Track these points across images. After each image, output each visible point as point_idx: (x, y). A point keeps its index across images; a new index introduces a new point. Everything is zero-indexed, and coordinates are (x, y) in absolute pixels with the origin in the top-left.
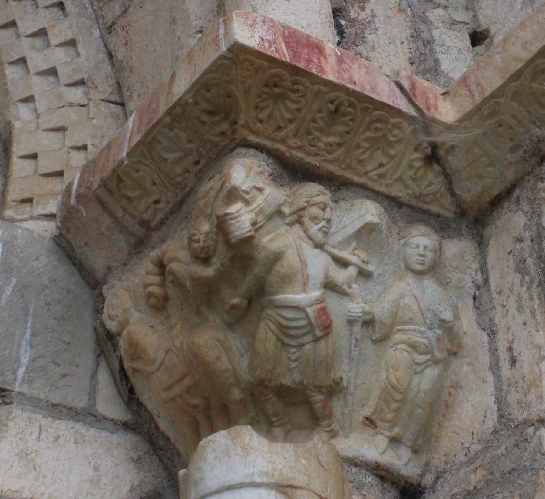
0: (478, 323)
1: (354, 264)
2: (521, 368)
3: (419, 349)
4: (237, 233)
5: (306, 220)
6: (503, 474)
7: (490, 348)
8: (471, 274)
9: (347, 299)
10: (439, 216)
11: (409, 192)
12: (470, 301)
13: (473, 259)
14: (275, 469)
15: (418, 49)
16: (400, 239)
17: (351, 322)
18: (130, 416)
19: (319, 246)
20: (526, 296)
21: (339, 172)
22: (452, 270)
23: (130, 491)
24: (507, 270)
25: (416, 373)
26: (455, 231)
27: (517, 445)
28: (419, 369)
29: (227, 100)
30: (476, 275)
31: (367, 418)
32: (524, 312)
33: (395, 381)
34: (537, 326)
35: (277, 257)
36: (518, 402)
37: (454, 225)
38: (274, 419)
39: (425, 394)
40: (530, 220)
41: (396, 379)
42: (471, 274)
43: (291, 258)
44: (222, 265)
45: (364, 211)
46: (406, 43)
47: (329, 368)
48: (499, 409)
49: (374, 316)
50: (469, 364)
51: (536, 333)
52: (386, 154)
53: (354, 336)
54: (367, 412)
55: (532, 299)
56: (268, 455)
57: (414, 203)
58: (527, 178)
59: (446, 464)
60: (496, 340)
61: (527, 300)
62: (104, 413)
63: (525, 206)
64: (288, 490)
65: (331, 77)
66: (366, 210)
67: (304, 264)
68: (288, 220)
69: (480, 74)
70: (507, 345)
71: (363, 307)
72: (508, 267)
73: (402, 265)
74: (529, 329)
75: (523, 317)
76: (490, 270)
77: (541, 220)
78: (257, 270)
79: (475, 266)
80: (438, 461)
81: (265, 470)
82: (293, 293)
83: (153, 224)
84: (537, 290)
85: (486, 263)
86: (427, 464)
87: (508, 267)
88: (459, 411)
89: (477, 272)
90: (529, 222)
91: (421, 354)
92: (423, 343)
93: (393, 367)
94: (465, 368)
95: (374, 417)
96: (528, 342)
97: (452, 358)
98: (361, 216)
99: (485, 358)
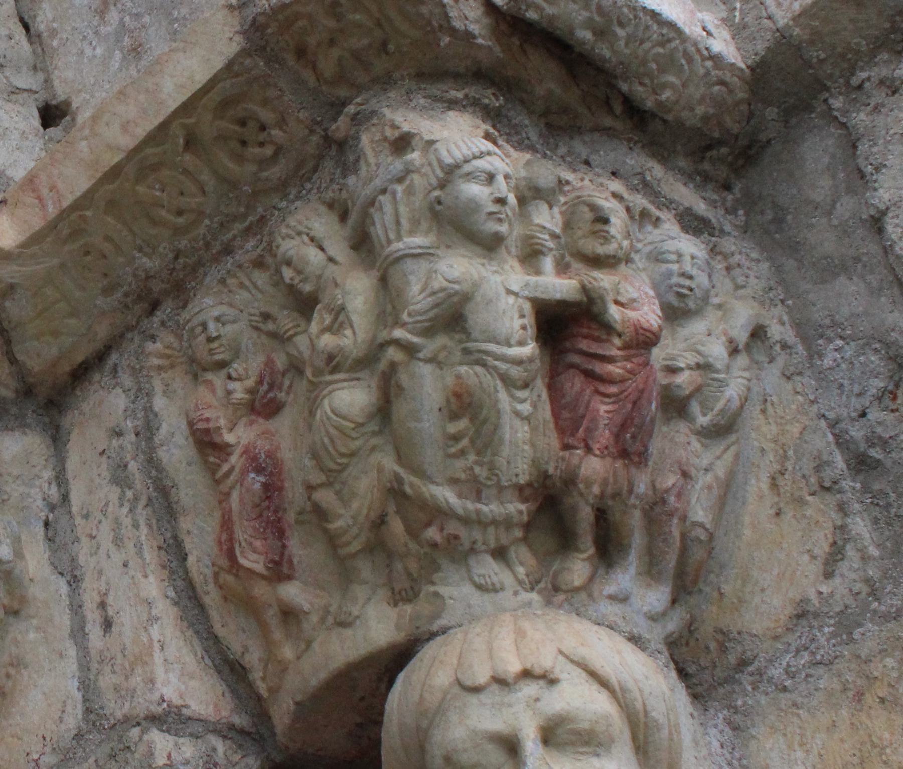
0: (52, 564)
2: (120, 635)
7: (71, 604)
8: (40, 487)
12: (40, 530)
13: (44, 463)
20: (127, 522)
22: (10, 480)
24: (98, 480)
26: (16, 418)
30: (49, 488)
32: (124, 547)
34: (144, 568)
37: (14, 410)
40: (134, 402)
42: (40, 487)
51: (143, 579)
55: (136, 526)
60: (81, 591)
61: (130, 528)
63: (127, 380)
70: (98, 599)
72: (99, 475)
74: (132, 573)
75: (124, 555)
76: (71, 481)
77: (151, 402)
79: (48, 474)
84: (145, 512)
85: (64, 469)
87: (99, 475)
89: (50, 484)
90: (132, 405)
96: (131, 594)
97: (11, 619)
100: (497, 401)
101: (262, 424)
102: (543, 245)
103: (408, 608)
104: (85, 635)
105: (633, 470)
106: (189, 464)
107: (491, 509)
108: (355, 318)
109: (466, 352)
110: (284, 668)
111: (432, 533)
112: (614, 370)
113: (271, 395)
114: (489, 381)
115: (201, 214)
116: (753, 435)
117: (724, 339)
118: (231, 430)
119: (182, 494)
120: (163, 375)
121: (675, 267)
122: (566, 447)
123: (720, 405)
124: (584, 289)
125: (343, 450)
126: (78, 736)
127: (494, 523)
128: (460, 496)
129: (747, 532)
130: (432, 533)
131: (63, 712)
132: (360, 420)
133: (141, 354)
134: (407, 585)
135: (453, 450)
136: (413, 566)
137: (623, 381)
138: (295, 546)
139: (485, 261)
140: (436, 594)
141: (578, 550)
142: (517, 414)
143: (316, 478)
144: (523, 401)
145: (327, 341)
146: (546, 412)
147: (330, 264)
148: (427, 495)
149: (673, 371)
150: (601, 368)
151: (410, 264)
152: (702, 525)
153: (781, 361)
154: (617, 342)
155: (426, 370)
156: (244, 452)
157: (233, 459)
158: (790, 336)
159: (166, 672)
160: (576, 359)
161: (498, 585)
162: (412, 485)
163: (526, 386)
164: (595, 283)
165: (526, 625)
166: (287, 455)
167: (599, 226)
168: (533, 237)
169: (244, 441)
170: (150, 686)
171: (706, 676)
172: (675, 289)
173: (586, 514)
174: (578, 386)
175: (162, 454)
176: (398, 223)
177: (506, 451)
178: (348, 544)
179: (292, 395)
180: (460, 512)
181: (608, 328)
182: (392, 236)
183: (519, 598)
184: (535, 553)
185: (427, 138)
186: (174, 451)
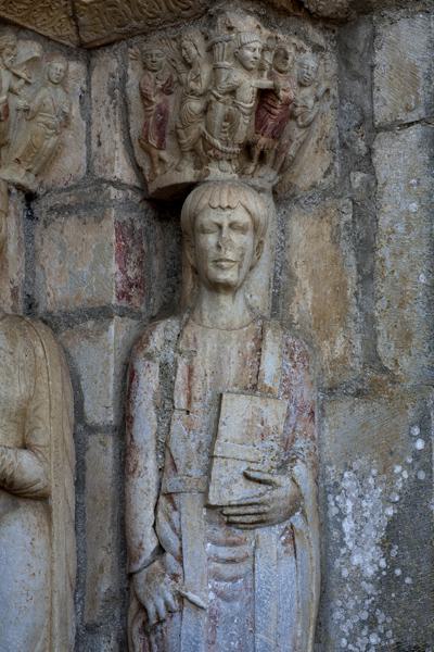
10: (68, 46)
17: (18, 110)
19: (8, 69)
20: (112, 111)
21: (22, 23)
27: (96, 190)
52: (48, 14)
73: (46, 77)
80: (48, 182)
86: (42, 182)
101: (165, 96)
103: (199, 171)
107: (229, 149)
110: (156, 175)
111: (211, 152)
112: (277, 112)
115: (159, 17)
129: (306, 155)
130: (211, 152)
133: (126, 51)
136: (204, 161)
138: (168, 140)
143: (179, 125)
145: (192, 84)
146: (253, 121)
149: (296, 106)
150: (273, 110)
151: (223, 71)
155: (221, 105)
157: (154, 107)
165: (232, 190)
173: (257, 153)
175: (128, 90)
181: (278, 98)
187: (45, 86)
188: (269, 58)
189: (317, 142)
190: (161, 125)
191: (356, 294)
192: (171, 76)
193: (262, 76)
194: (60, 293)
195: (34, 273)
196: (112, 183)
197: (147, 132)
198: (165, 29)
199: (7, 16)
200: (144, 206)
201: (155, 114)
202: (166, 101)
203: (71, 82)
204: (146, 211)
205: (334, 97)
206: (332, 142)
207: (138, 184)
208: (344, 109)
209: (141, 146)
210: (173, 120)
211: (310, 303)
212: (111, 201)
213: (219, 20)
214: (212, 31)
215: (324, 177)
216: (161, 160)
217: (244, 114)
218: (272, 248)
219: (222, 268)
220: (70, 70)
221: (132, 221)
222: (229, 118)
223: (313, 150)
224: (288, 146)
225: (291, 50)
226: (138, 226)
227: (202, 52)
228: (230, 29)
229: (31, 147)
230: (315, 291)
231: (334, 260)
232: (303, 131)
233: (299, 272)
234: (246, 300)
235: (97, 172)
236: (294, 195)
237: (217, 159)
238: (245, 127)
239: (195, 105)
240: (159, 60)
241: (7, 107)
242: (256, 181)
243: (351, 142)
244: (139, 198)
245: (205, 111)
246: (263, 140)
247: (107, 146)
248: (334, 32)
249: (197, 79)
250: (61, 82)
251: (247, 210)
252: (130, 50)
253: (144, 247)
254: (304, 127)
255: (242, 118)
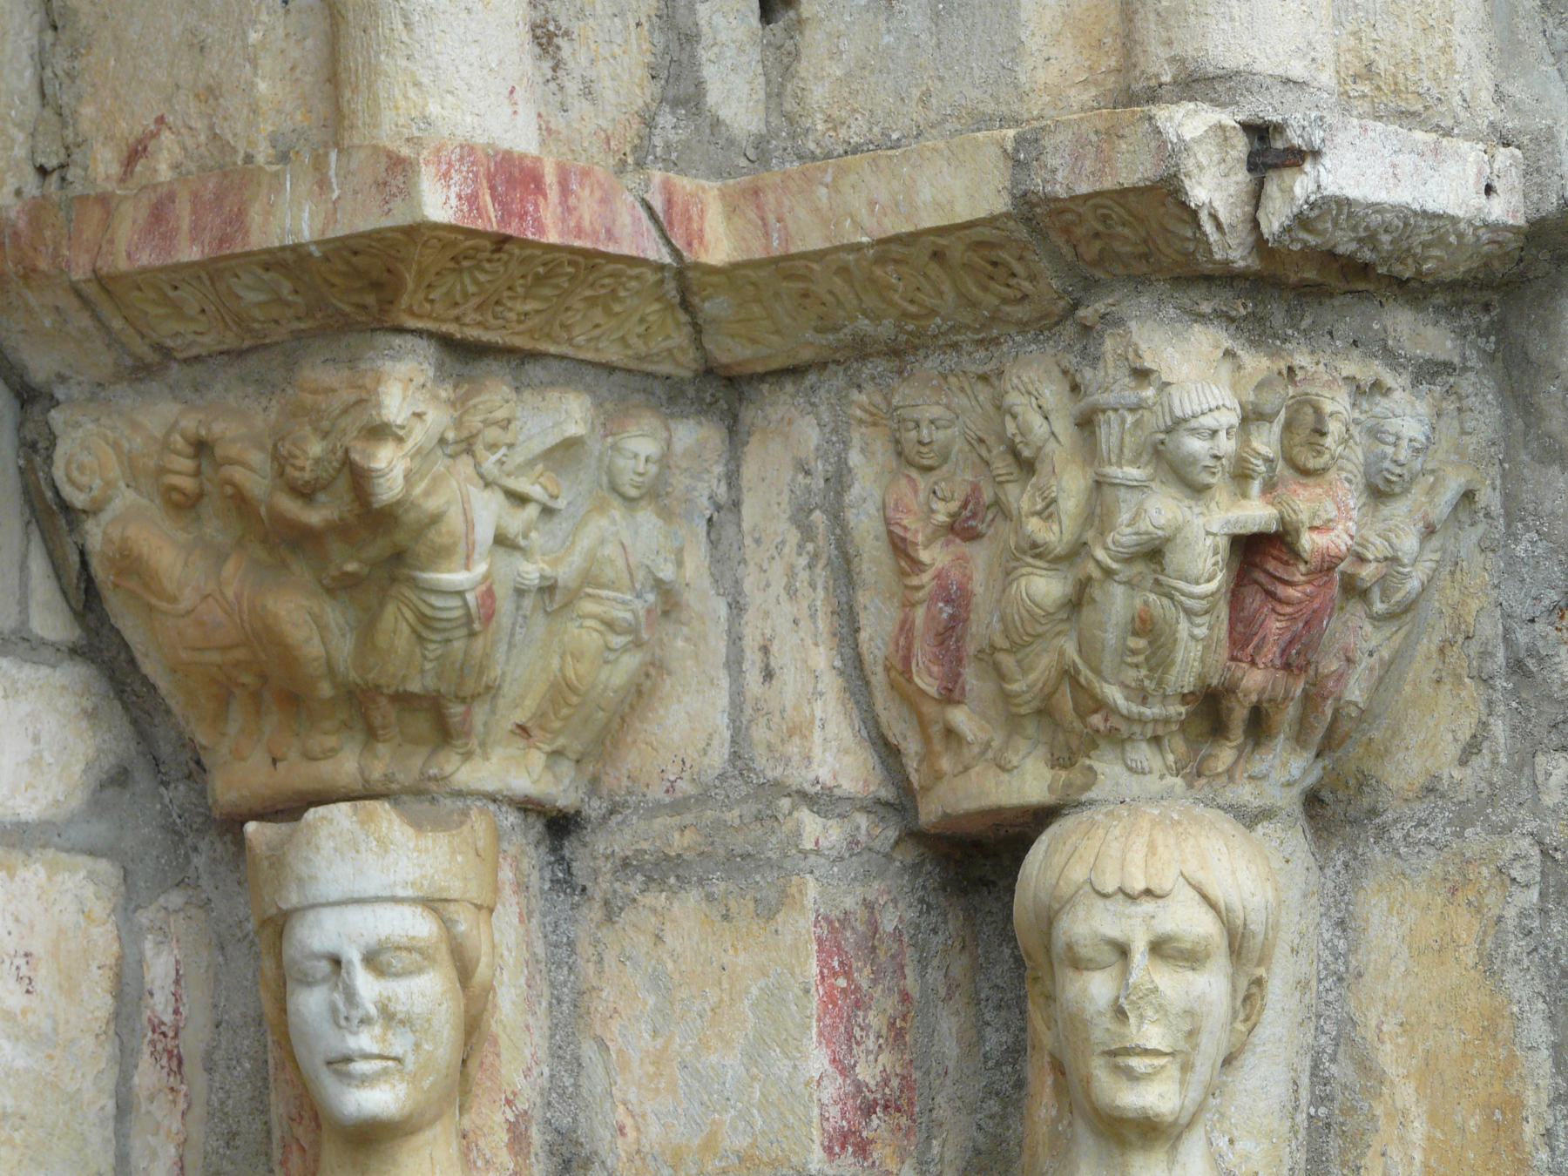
0: (712, 575)
1: (537, 501)
3: (618, 629)
4: (385, 497)
5: (479, 448)
6: (731, 856)
9: (518, 554)
11: (630, 352)
12: (702, 528)
14: (424, 877)
15: (666, 50)
16: (606, 436)
17: (520, 592)
18: (78, 632)
20: (804, 575)
23: (85, 771)
24: (775, 509)
25: (606, 662)
26: (692, 403)
27: (758, 818)
28: (612, 656)
29: (385, 274)
30: (718, 487)
31: (519, 726)
33: (573, 677)
35: (435, 519)
36: (769, 746)
38: (381, 732)
39: (615, 692)
41: (576, 674)
43: (454, 520)
44: (341, 519)
45: (564, 416)
46: (646, 26)
47: (482, 670)
48: (733, 742)
49: (556, 581)
50: (687, 639)
51: (813, 647)
53: (521, 613)
54: (520, 716)
56: (415, 854)
57: (633, 365)
58: (833, 367)
59: (630, 793)
60: (743, 622)
61: (806, 584)
62: (41, 633)
64: (440, 906)
65: (553, 237)
66: (566, 411)
67: (470, 524)
68: (449, 450)
69: (787, 202)
70: (760, 640)
71: (543, 569)
72: (779, 504)
73: (605, 479)
74: (802, 634)
76: (745, 490)
78: (401, 537)
79: (719, 469)
81: (411, 878)
82: (449, 571)
83: (179, 356)
87: (779, 504)
88: (661, 712)
89: (719, 481)
91: (618, 634)
92: (624, 619)
93: (573, 655)
94: (680, 643)
95: (529, 725)
98: (557, 424)
99: (719, 645)
100: (1176, 631)
102: (1254, 471)
103: (1063, 774)
104: (741, 671)
105: (1291, 680)
106: (877, 538)
108: (1064, 519)
109: (1157, 582)
110: (939, 776)
111: (1096, 720)
112: (1292, 593)
113: (973, 523)
114: (1171, 611)
116: (1436, 597)
117: (1421, 524)
118: (926, 547)
119: (864, 567)
120: (863, 430)
121: (1390, 450)
122: (1233, 658)
123: (1398, 596)
124: (1282, 520)
125: (1030, 630)
126: (722, 777)
127: (1155, 721)
128: (1127, 699)
129: (1408, 689)
131: (708, 745)
132: (1052, 610)
134: (1066, 755)
135: (1129, 660)
136: (1075, 743)
137: (1300, 602)
139: (1192, 503)
140: (1090, 768)
141: (1227, 739)
142: (1193, 637)
143: (1000, 641)
144: (1199, 626)
145: (1034, 525)
147: (1052, 445)
148: (1098, 691)
149: (1362, 559)
150: (1282, 590)
151: (1122, 493)
152: (1356, 704)
153: (1481, 528)
154: (1302, 568)
155: (1119, 591)
156: (938, 576)
157: (925, 578)
158: (1496, 508)
159: (824, 751)
160: (1262, 577)
161: (1147, 770)
162: (1086, 679)
163: (1207, 612)
164: (1294, 517)
165: (1159, 838)
166: (978, 586)
167: (1317, 438)
168: (1246, 460)
169: (939, 565)
170: (806, 762)
171: (1340, 809)
172: (1386, 474)
174: (1256, 605)
175: (850, 516)
176: (1121, 450)
177: (1174, 671)
178: (1020, 705)
179: (992, 529)
180: (1125, 712)
181: (1297, 555)
182: (1114, 459)
183: (1164, 782)
184: (1186, 740)
185: (1164, 379)
186: (863, 518)
187: (601, 508)
188: (1266, 442)
189: (1442, 651)
190: (950, 634)
191: (1549, 1134)
192: (976, 488)
193: (1245, 496)
194: (654, 1130)
195: (577, 1060)
196: (806, 798)
197: (909, 648)
198: (955, 346)
199: (487, 336)
200: (909, 854)
201: (933, 599)
202: (961, 559)
203: (679, 482)
204: (915, 869)
205: (1487, 515)
206: (1485, 654)
207: (886, 793)
208: (1520, 550)
209: (893, 686)
210: (983, 625)
211: (1418, 1157)
212: (805, 854)
213: (1109, 344)
214: (1088, 373)
215: (1463, 762)
216: (950, 733)
217: (1189, 613)
218: (1302, 985)
219: (1132, 1076)
220: (678, 447)
221: (869, 905)
222: (1144, 626)
223: (1428, 674)
224: (1340, 677)
225: (1337, 404)
226: (889, 922)
227: (1063, 427)
228: (1142, 375)
229: (561, 692)
230: (1434, 1118)
231: (1489, 1031)
232: (1388, 630)
233: (1388, 1057)
234: (1216, 1158)
235: (762, 762)
236: (1373, 812)
237: (1117, 739)
238: (1196, 650)
239: (1046, 587)
240: (940, 436)
241: (489, 594)
242: (1244, 793)
243: (1541, 660)
244: (892, 834)
245: (1077, 602)
246: (1254, 680)
247: (790, 683)
248: (1487, 308)
249: (1048, 511)
250: (655, 493)
251: (1205, 897)
252: (855, 395)
253: (911, 983)
254: (1390, 617)
255: (1183, 626)
